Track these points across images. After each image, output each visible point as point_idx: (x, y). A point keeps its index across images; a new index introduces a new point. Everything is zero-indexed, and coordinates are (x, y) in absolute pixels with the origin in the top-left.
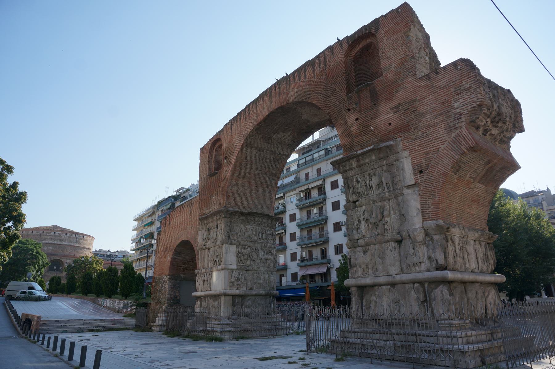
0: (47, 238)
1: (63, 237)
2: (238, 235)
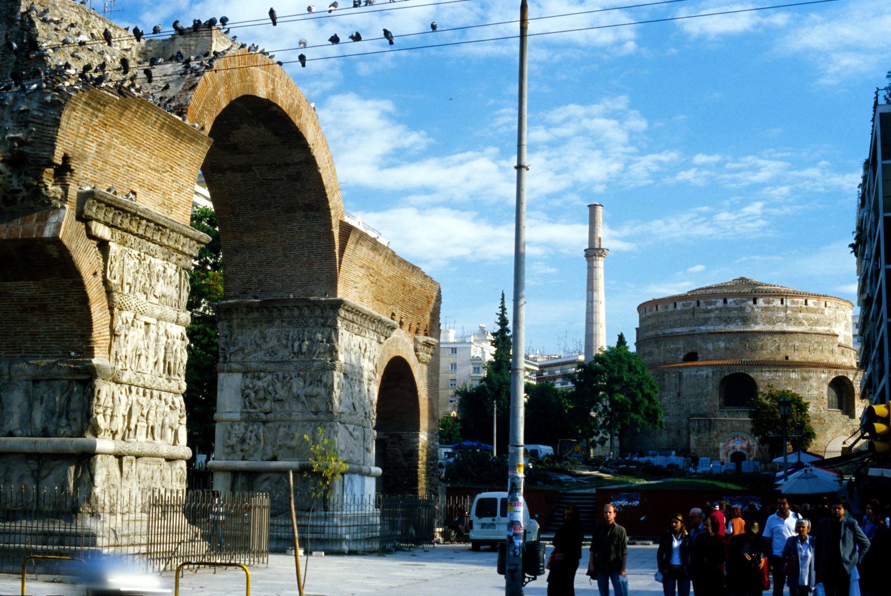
0: (709, 318)
1: (748, 310)
2: (246, 351)
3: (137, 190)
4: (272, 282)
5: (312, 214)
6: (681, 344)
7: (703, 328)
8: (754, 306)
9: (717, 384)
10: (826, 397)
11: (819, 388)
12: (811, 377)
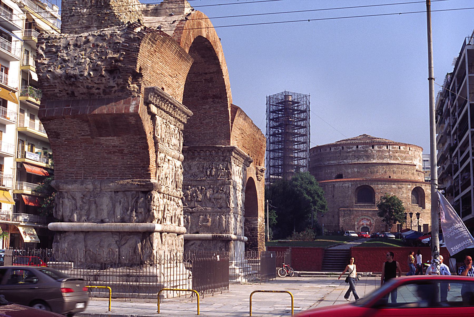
3: (164, 87)
4: (193, 137)
5: (217, 100)
10: (411, 197)
11: (407, 193)
12: (403, 187)
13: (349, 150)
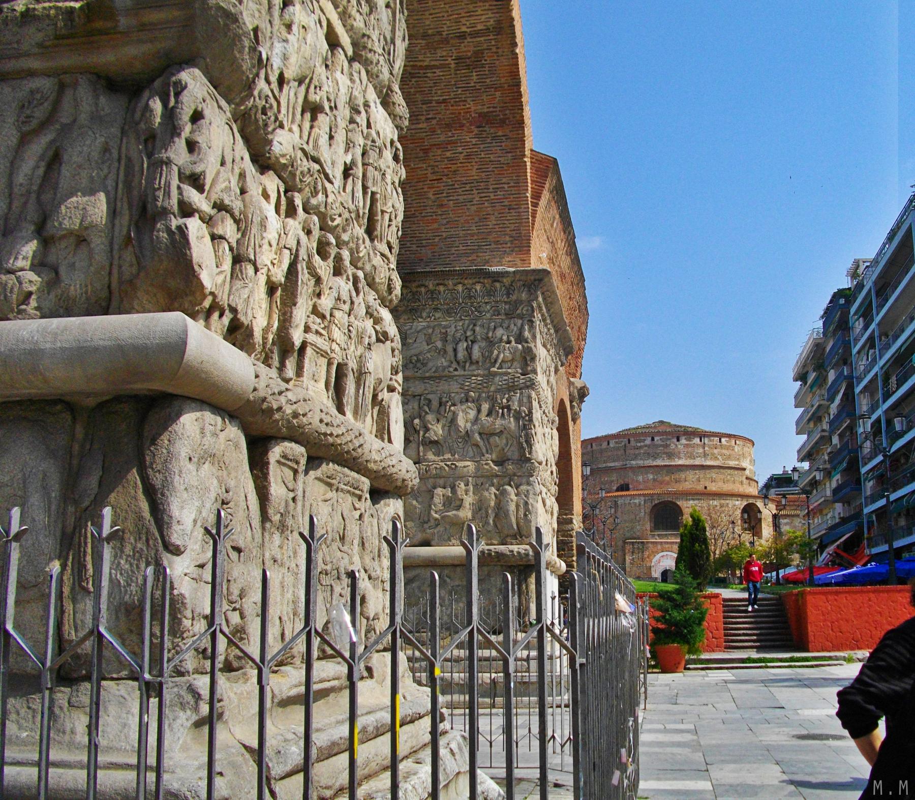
4: (414, 247)
6: (614, 477)
7: (633, 462)
8: (677, 443)
9: (648, 511)
13: (639, 444)
